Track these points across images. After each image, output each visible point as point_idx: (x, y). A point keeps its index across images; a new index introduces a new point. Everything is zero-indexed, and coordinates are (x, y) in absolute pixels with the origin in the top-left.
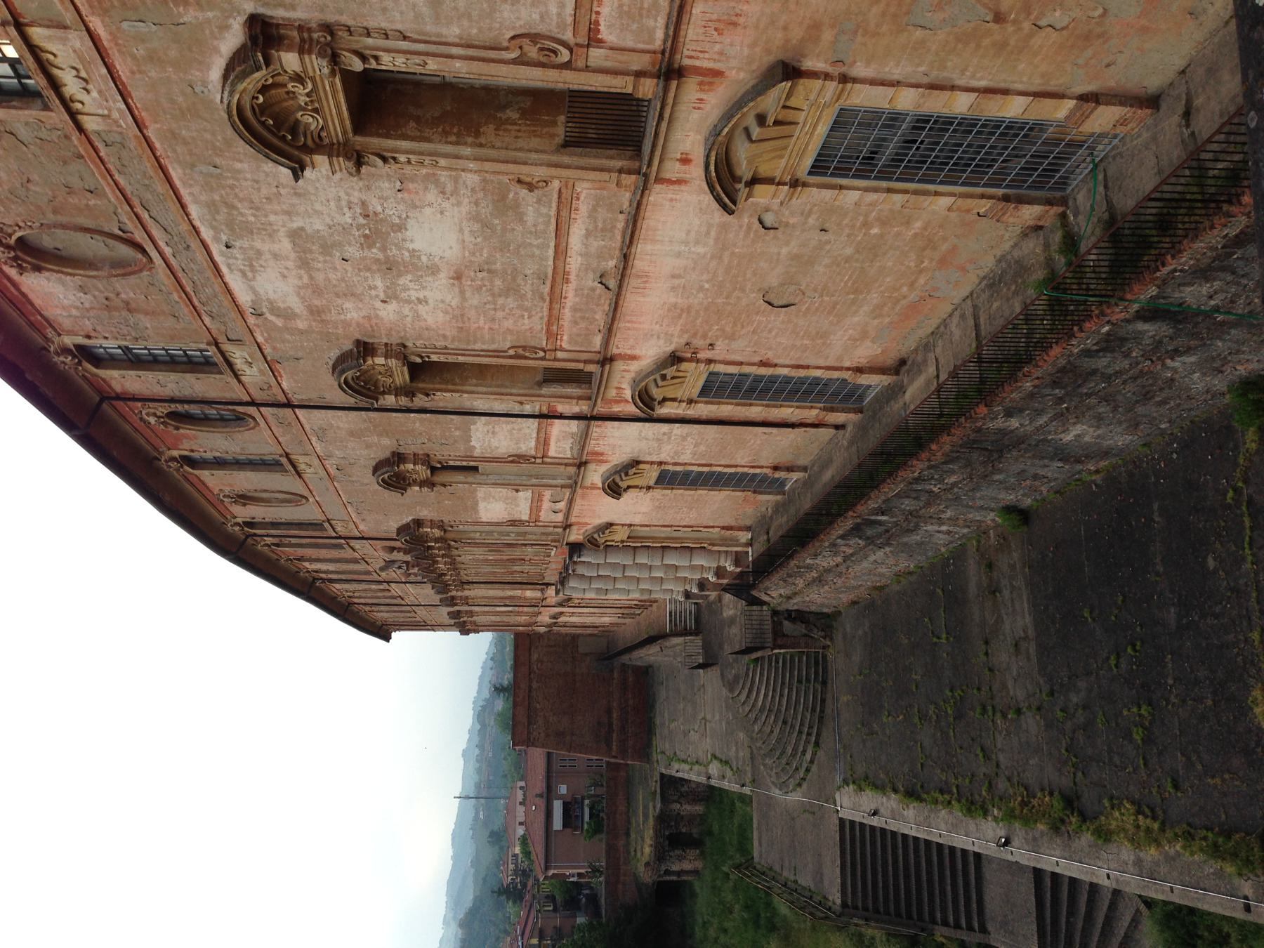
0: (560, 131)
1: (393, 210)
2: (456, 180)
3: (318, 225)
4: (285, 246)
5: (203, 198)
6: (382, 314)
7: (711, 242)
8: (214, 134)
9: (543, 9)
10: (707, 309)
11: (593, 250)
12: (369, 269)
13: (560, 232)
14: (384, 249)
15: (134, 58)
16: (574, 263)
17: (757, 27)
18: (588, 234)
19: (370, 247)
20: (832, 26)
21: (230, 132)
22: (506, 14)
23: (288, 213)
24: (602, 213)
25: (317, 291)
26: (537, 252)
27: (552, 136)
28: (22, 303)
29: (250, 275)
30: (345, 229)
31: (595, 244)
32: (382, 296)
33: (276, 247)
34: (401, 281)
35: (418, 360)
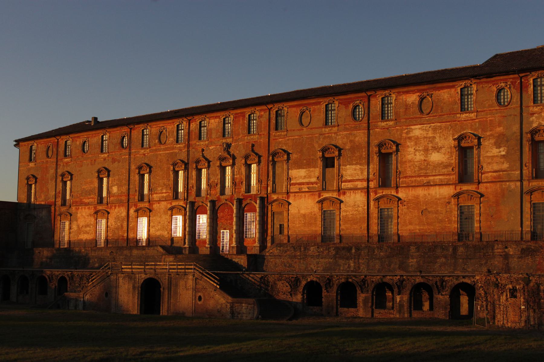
1: (443, 150)
3: (437, 140)
4: (430, 134)
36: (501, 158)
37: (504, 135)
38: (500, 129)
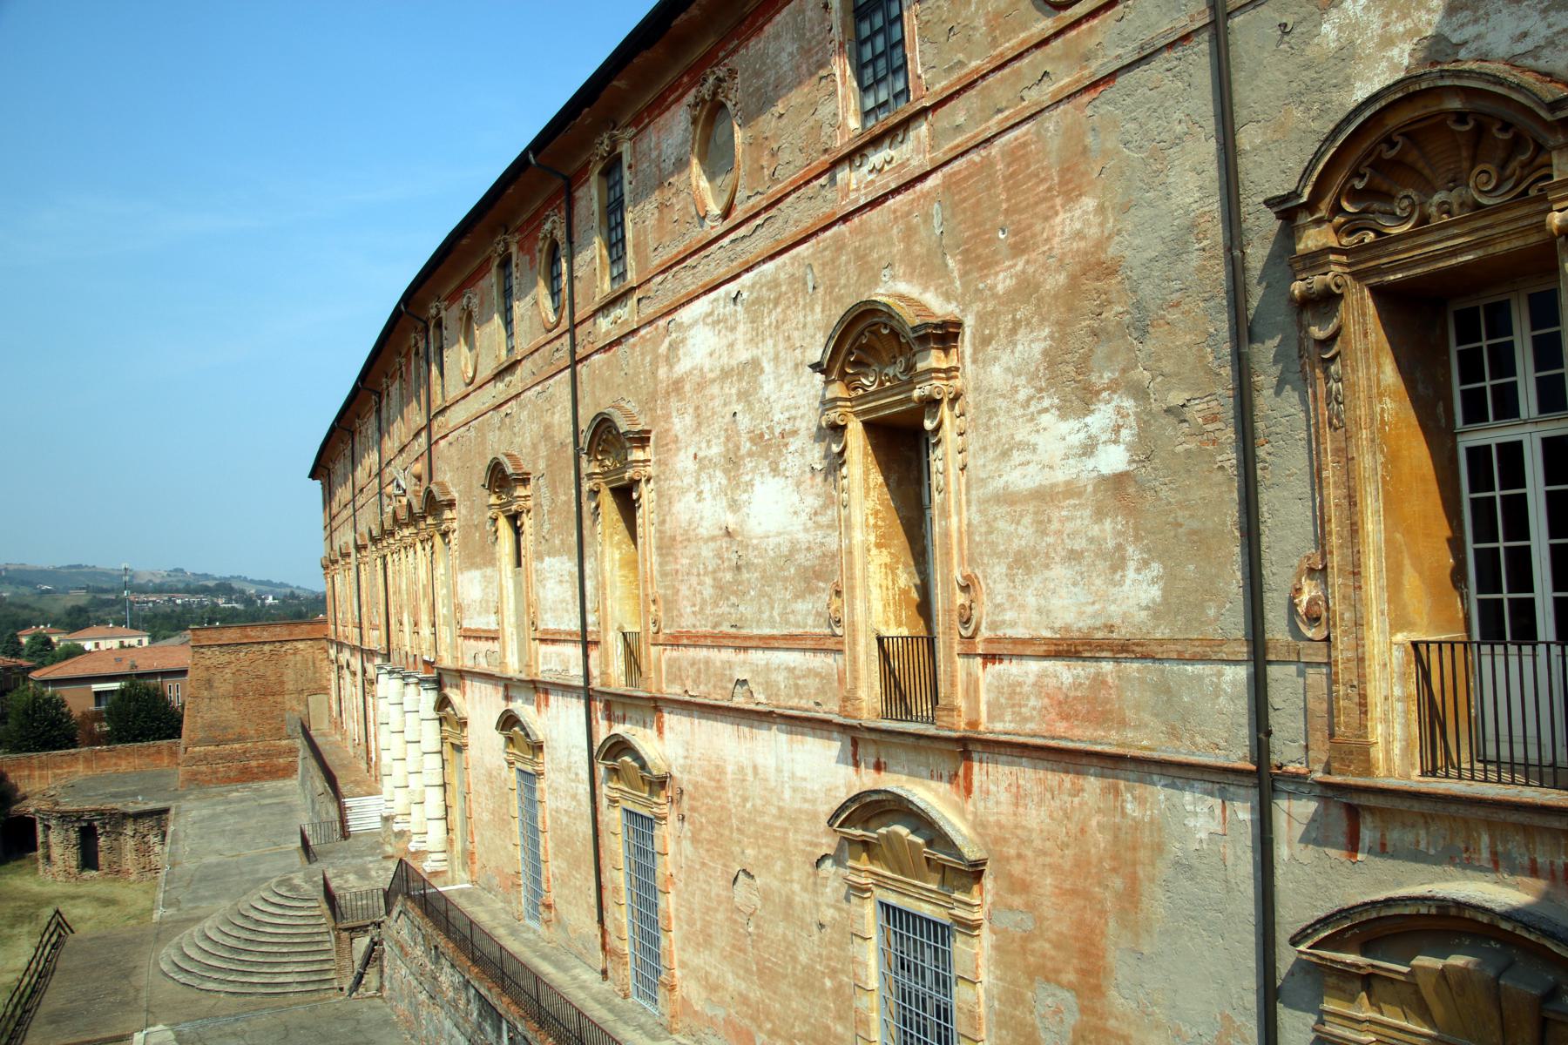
0: (892, 631)
2: (829, 526)
3: (768, 386)
4: (743, 354)
5: (782, 276)
6: (682, 454)
7: (797, 805)
8: (845, 286)
9: (1007, 605)
10: (723, 808)
11: (773, 676)
12: (728, 439)
13: (791, 642)
14: (750, 454)
15: (909, 213)
16: (758, 657)
17: (1016, 827)
18: (791, 670)
19: (752, 440)
20: (1027, 905)
21: (850, 302)
22: (997, 569)
23: (776, 358)
24: (813, 684)
25: (700, 387)
26: (765, 616)
27: (887, 624)
28: (659, 106)
29: (709, 320)
30: (766, 415)
31: (780, 678)
32: (701, 454)
33: (740, 345)
34: (719, 473)
35: (635, 496)
36: (1099, 514)
37: (1109, 270)
38: (1073, 223)
